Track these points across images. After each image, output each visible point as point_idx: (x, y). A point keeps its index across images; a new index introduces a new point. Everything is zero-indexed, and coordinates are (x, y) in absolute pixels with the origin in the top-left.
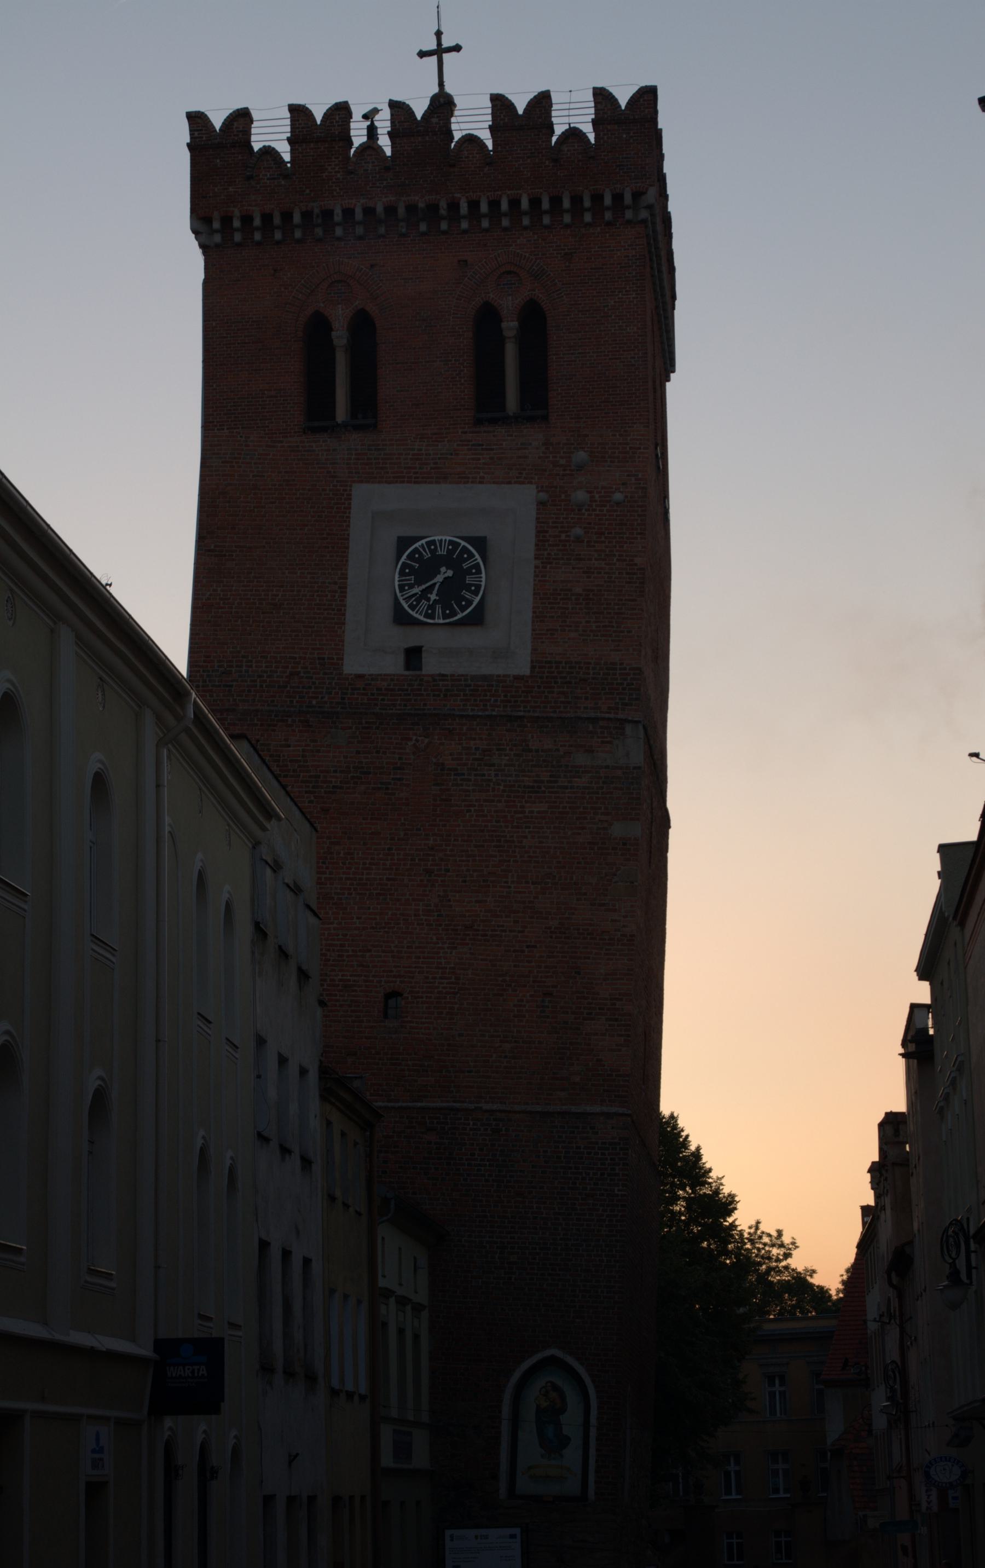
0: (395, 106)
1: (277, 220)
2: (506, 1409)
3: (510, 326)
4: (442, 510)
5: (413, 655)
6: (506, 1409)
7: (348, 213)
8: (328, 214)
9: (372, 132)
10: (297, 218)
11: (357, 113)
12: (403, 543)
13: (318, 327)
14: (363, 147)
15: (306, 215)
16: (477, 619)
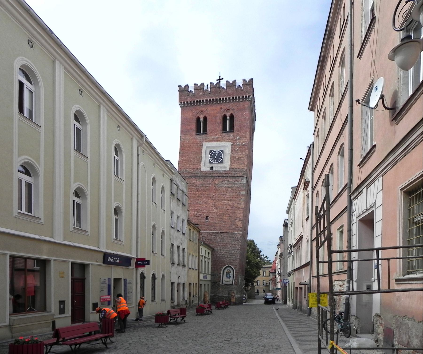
0: (211, 83)
1: (192, 102)
2: (222, 273)
3: (228, 118)
4: (216, 146)
5: (212, 168)
6: (222, 273)
7: (203, 101)
8: (200, 101)
9: (207, 88)
10: (195, 102)
11: (206, 85)
12: (211, 151)
13: (198, 119)
14: (206, 90)
15: (197, 101)
16: (221, 162)
